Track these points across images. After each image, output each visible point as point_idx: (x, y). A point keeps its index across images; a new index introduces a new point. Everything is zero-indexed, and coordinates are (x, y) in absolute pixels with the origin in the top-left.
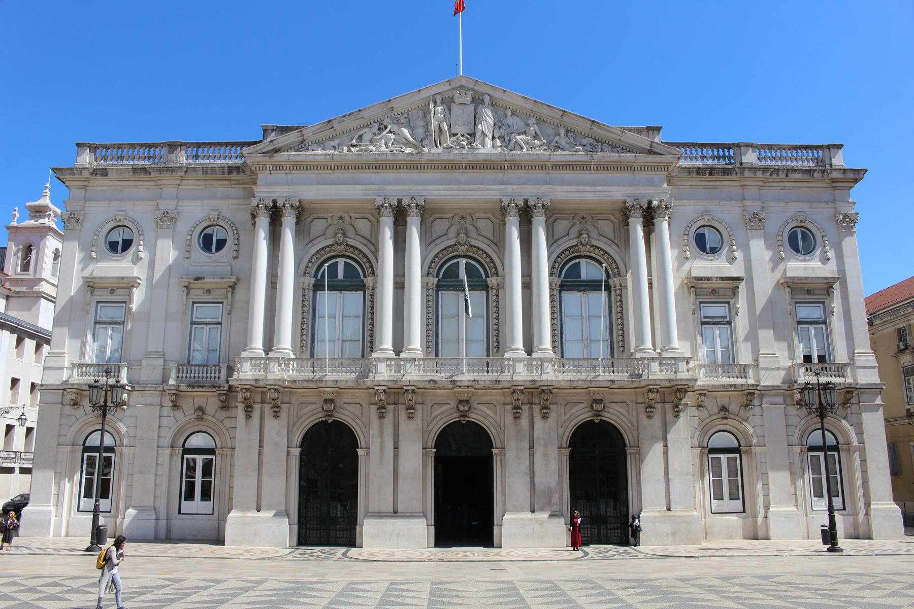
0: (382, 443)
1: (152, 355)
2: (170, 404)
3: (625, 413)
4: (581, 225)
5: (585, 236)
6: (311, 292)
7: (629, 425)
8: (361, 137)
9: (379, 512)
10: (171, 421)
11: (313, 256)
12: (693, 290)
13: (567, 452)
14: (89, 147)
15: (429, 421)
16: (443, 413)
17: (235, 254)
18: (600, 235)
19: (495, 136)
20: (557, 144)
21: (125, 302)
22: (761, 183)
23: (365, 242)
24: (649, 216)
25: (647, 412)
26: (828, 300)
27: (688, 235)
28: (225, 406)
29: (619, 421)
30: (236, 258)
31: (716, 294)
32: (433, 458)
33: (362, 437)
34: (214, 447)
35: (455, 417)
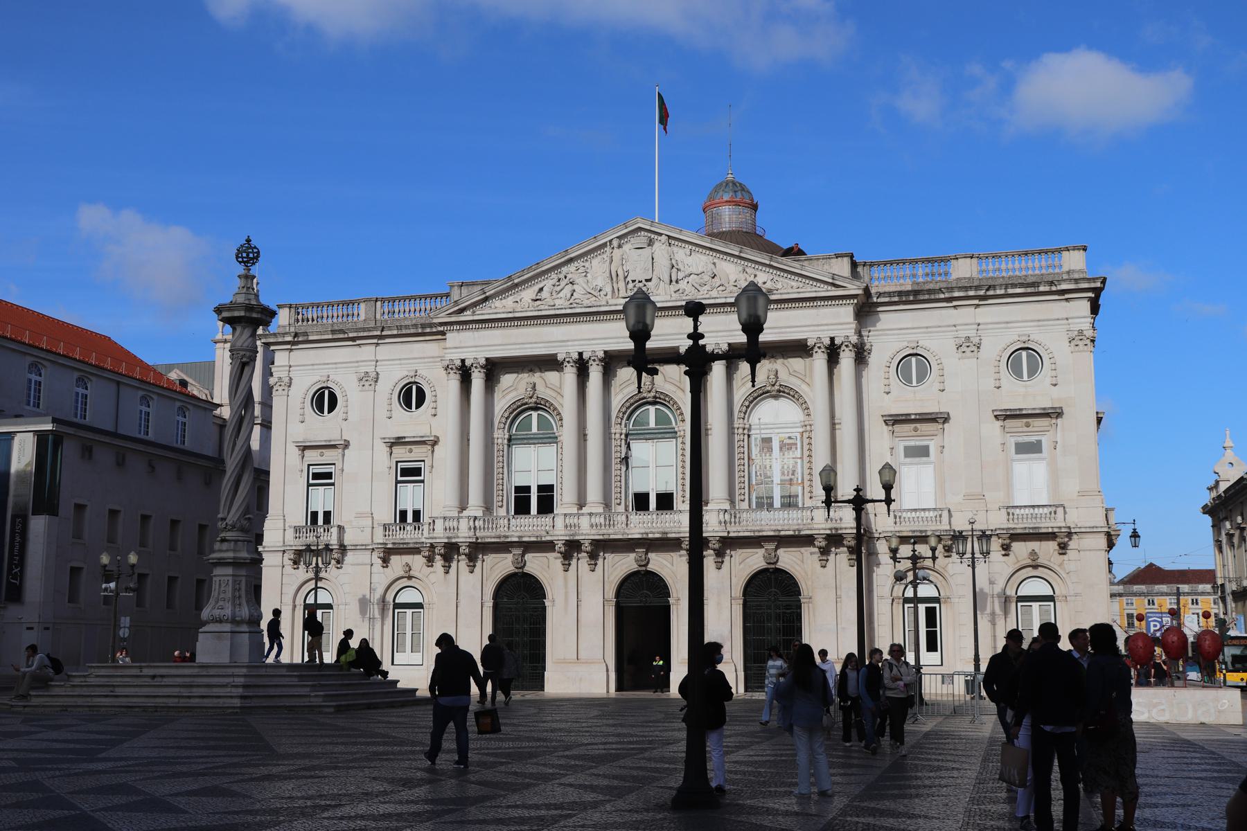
0: (566, 594)
1: (360, 516)
2: (380, 561)
3: (799, 562)
4: (771, 364)
5: (772, 377)
6: (506, 447)
7: (803, 574)
8: (541, 290)
9: (564, 659)
10: (382, 577)
11: (506, 410)
12: (890, 428)
13: (741, 602)
14: (290, 308)
15: (610, 572)
16: (623, 564)
17: (433, 412)
18: (790, 374)
19: (674, 279)
20: (735, 284)
21: (334, 464)
22: (976, 302)
23: (554, 394)
24: (833, 353)
25: (820, 560)
26: (1051, 432)
27: (889, 367)
28: (430, 560)
29: (793, 570)
30: (435, 415)
31: (919, 432)
32: (614, 607)
33: (548, 588)
34: (421, 601)
35: (634, 567)
